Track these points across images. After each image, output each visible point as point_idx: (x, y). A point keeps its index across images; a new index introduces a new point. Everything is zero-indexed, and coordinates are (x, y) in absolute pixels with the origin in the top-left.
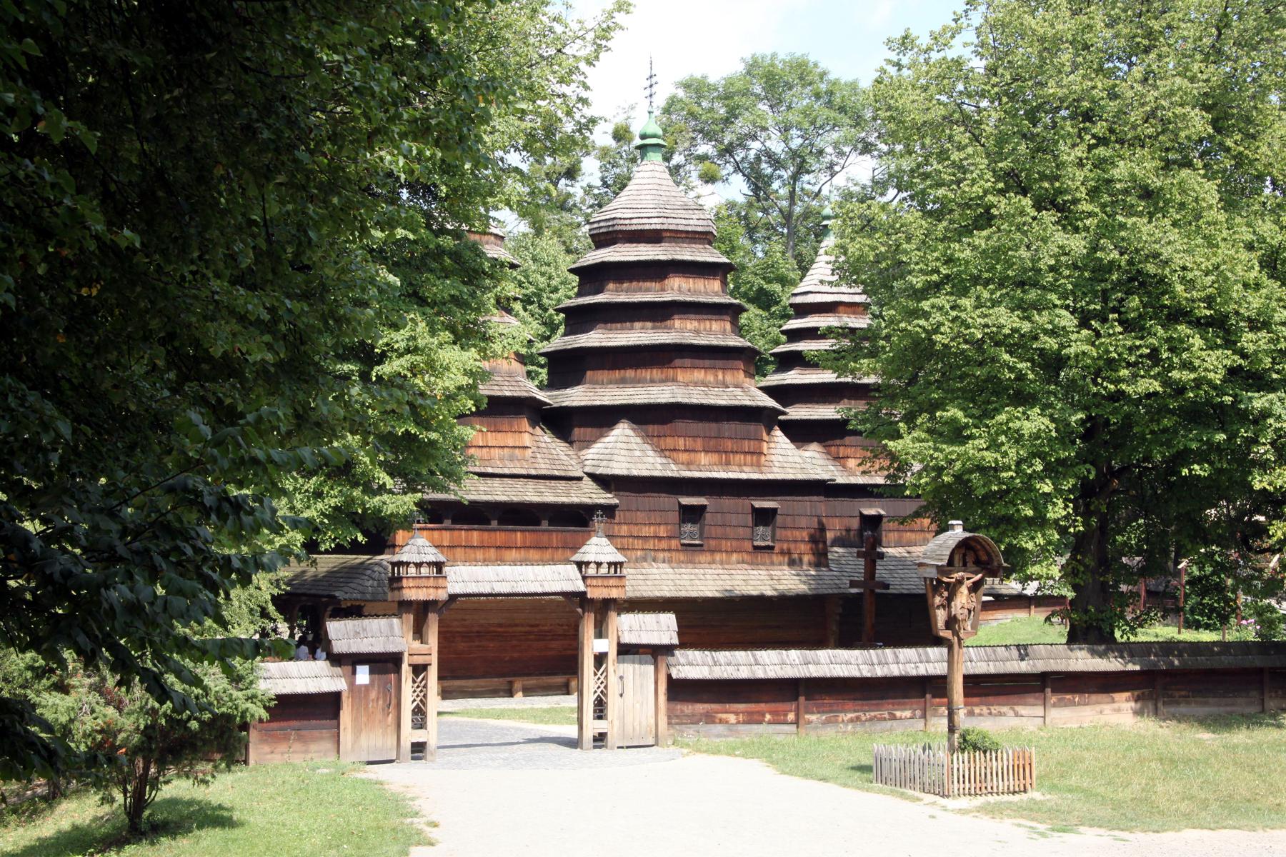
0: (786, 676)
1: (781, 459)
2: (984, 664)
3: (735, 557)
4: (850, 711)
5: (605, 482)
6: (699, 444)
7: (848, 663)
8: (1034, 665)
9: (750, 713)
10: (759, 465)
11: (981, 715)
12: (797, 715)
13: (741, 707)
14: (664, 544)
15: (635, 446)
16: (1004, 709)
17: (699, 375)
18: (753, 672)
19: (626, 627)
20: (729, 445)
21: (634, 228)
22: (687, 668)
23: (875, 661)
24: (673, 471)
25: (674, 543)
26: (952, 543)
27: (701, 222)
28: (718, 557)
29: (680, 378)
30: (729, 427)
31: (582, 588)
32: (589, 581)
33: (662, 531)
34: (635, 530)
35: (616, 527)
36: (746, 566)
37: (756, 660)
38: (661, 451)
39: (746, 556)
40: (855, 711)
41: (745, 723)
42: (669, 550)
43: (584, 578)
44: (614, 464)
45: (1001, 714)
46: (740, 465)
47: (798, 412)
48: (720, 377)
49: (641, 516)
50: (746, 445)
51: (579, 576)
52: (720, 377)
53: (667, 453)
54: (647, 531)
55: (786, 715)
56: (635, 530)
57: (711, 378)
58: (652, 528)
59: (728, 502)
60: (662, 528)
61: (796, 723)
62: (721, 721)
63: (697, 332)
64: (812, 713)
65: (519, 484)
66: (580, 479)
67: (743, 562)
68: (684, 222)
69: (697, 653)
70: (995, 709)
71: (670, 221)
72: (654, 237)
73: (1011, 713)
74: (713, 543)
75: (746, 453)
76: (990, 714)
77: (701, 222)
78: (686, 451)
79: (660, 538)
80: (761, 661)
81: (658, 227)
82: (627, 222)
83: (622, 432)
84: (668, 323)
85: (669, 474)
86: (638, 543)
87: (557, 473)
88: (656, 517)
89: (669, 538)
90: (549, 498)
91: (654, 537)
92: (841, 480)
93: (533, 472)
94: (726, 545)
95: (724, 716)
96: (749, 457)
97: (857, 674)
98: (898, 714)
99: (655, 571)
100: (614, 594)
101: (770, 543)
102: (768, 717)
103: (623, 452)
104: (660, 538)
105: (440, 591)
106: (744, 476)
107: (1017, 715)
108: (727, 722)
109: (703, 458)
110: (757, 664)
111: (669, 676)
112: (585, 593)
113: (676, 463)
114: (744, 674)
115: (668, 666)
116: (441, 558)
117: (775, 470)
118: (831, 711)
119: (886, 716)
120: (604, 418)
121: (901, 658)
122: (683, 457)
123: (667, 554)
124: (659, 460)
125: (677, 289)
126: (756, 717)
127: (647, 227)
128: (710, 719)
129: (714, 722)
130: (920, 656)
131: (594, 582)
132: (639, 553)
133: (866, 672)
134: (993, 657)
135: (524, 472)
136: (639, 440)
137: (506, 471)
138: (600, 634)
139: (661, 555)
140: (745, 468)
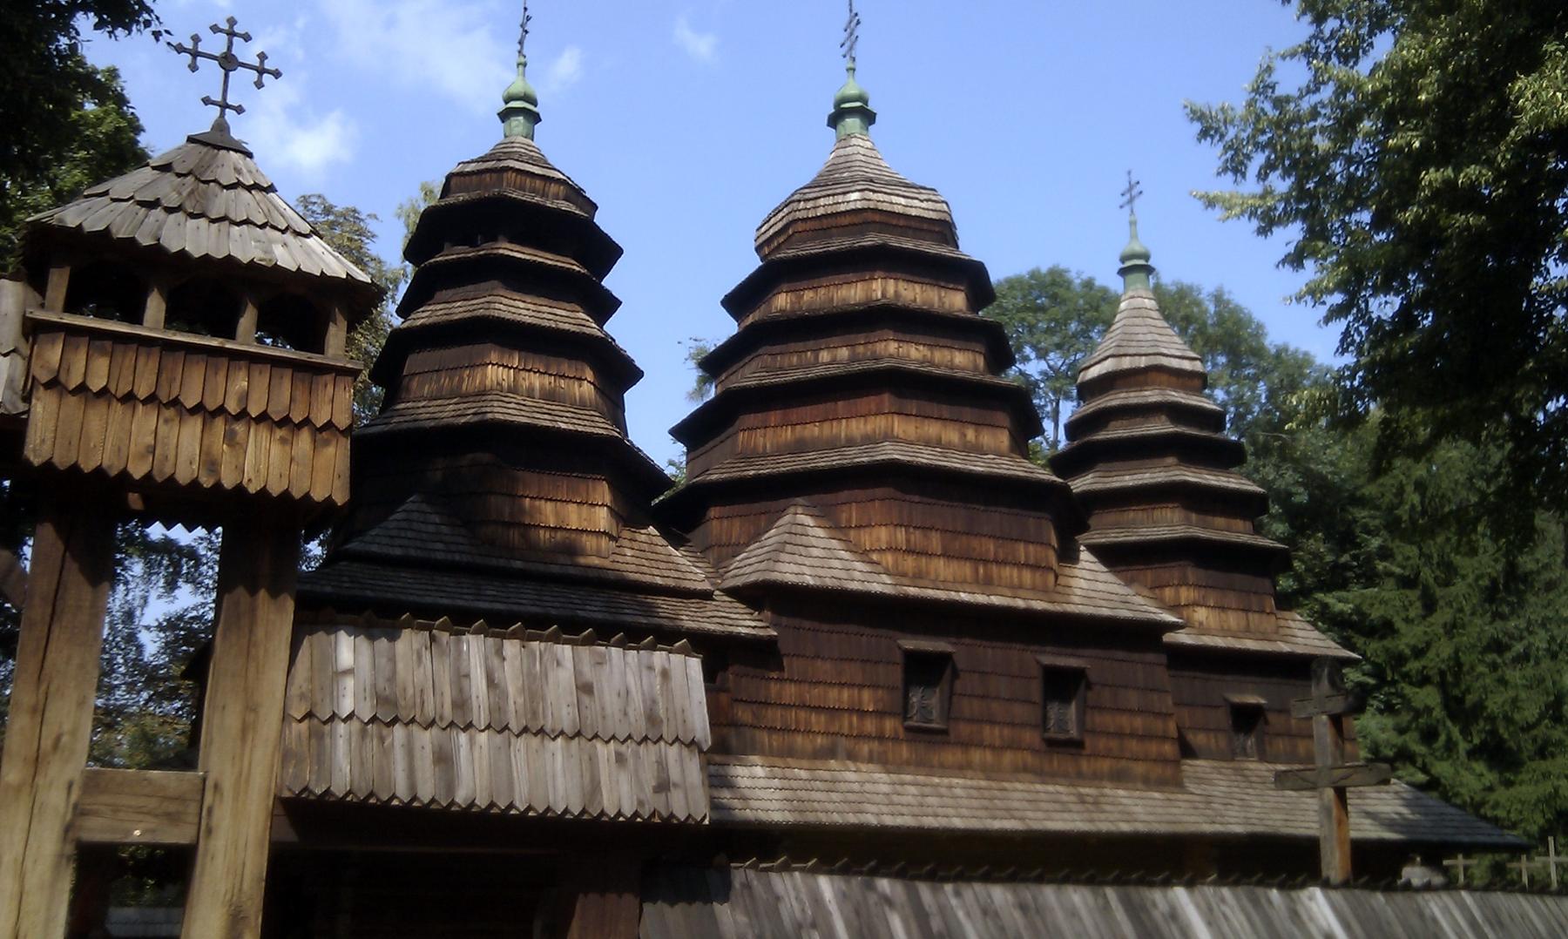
1: (1083, 584)
3: (1008, 758)
6: (936, 541)
10: (1045, 591)
14: (870, 726)
15: (814, 541)
21: (820, 212)
24: (881, 585)
25: (890, 725)
28: (977, 756)
30: (996, 518)
33: (868, 699)
34: (814, 694)
36: (1030, 777)
38: (863, 554)
39: (1029, 758)
42: (880, 738)
46: (1012, 587)
49: (824, 668)
53: (875, 557)
54: (835, 696)
56: (814, 694)
57: (951, 434)
58: (846, 694)
59: (991, 653)
66: (706, 596)
67: (1025, 769)
68: (903, 201)
69: (826, 886)
71: (881, 197)
74: (964, 730)
78: (909, 551)
79: (862, 713)
81: (859, 205)
82: (809, 205)
85: (876, 588)
86: (818, 721)
87: (659, 581)
88: (852, 671)
89: (879, 714)
91: (850, 711)
94: (991, 733)
96: (1027, 576)
101: (1074, 733)
104: (862, 713)
109: (942, 568)
117: (1076, 599)
122: (909, 563)
123: (875, 745)
124: (859, 565)
127: (842, 208)
132: (819, 740)
136: (820, 532)
139: (865, 748)
140: (1021, 593)
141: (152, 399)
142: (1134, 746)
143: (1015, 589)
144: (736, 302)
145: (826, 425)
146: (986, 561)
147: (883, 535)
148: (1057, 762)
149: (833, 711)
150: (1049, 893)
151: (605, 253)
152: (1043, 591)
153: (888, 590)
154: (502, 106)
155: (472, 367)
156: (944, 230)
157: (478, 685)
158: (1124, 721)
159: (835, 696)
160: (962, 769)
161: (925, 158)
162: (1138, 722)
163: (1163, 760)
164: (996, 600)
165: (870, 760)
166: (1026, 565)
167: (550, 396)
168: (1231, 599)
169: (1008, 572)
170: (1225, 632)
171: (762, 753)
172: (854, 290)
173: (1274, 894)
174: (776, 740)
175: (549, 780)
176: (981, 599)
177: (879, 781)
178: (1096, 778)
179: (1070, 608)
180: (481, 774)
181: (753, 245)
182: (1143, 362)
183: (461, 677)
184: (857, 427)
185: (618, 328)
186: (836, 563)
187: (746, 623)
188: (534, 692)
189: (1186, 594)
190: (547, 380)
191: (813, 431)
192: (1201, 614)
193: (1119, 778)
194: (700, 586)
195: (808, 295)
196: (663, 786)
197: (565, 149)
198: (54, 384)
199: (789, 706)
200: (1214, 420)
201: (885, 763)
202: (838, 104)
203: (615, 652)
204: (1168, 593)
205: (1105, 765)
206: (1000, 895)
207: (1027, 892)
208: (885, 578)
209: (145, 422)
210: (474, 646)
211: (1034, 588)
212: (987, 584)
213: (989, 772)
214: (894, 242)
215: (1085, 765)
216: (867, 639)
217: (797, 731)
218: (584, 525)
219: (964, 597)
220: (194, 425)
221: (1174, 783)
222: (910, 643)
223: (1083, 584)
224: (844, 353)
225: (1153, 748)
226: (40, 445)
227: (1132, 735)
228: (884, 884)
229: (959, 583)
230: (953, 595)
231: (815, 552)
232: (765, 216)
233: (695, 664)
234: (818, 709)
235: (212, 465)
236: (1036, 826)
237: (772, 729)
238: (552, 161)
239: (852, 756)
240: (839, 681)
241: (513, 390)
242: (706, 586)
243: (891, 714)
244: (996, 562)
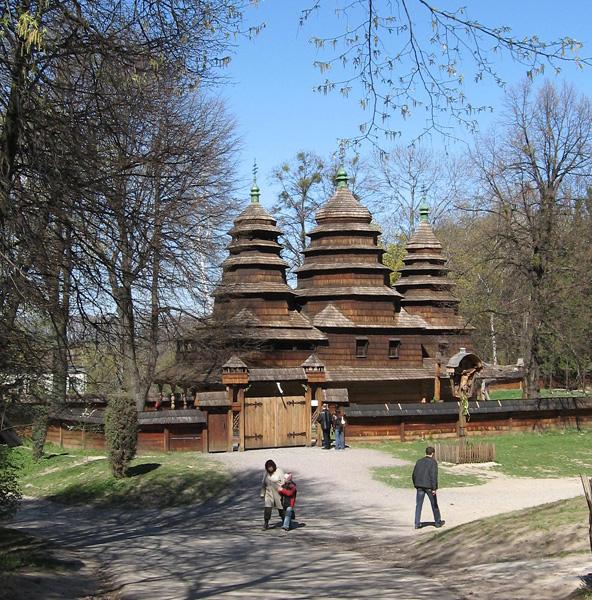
3: (380, 363)
5: (323, 329)
6: (364, 312)
20: (378, 312)
24: (351, 325)
26: (461, 358)
28: (373, 363)
33: (348, 351)
38: (347, 316)
47: (410, 297)
54: (342, 351)
59: (377, 338)
66: (311, 329)
74: (371, 356)
83: (330, 307)
92: (428, 328)
94: (376, 357)
100: (320, 380)
114: (378, 413)
122: (357, 318)
138: (313, 398)
139: (347, 362)
142: (411, 358)
147: (351, 312)
148: (394, 363)
152: (391, 323)
158: (409, 352)
159: (342, 351)
162: (412, 352)
176: (375, 326)
177: (350, 369)
182: (423, 246)
187: (321, 337)
189: (430, 315)
192: (433, 320)
200: (442, 262)
205: (404, 363)
212: (376, 322)
215: (399, 363)
216: (348, 337)
222: (357, 338)
224: (341, 259)
225: (416, 358)
240: (341, 344)
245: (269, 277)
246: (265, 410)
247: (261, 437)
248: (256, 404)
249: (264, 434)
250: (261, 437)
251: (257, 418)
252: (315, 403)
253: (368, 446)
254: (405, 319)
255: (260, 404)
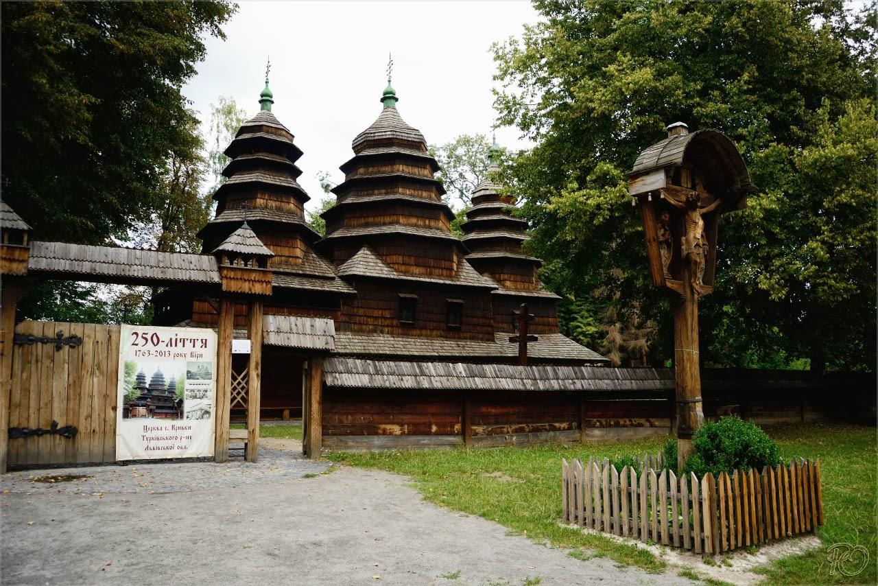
0: (452, 387)
1: (465, 274)
2: (628, 382)
3: (435, 332)
4: (514, 423)
5: (349, 279)
6: (412, 260)
7: (512, 377)
8: (665, 384)
9: (415, 425)
11: (624, 426)
12: (463, 427)
13: (406, 418)
14: (388, 322)
15: (370, 260)
16: (643, 421)
17: (414, 221)
18: (418, 383)
19: (272, 328)
21: (376, 138)
22: (345, 376)
23: (537, 376)
24: (394, 275)
25: (395, 322)
27: (417, 137)
29: (401, 221)
31: (216, 279)
32: (225, 272)
35: (355, 310)
37: (422, 371)
38: (388, 264)
40: (519, 423)
41: (410, 434)
42: (392, 326)
43: (220, 269)
44: (355, 269)
45: (640, 425)
46: (439, 276)
48: (427, 223)
50: (444, 264)
51: (215, 268)
52: (427, 223)
54: (376, 313)
55: (452, 427)
56: (369, 312)
57: (421, 223)
58: (380, 312)
60: (387, 312)
61: (463, 433)
62: (385, 433)
63: (411, 195)
64: (479, 425)
65: (288, 279)
66: (333, 279)
70: (636, 421)
72: (389, 142)
73: (648, 424)
74: (421, 323)
75: (442, 269)
76: (632, 425)
77: (417, 137)
78: (403, 264)
80: (427, 371)
84: (396, 190)
85: (392, 277)
86: (370, 321)
89: (392, 318)
90: (308, 286)
93: (301, 272)
95: (388, 427)
96: (444, 272)
97: (521, 387)
98: (557, 425)
99: (382, 338)
102: (434, 428)
103: (361, 263)
105: (15, 265)
106: (442, 282)
107: (652, 426)
108: (391, 434)
109: (416, 270)
110: (423, 374)
111: (324, 383)
112: (220, 285)
113: (396, 271)
114: (409, 383)
115: (323, 374)
116: (22, 225)
118: (497, 423)
119: (547, 427)
120: (352, 246)
121: (560, 373)
122: (403, 268)
123: (390, 328)
124: (386, 269)
125: (402, 170)
126: (423, 428)
127: (384, 137)
128: (372, 430)
129: (377, 434)
130: (576, 373)
131: (232, 275)
133: (529, 385)
134: (634, 376)
135: (294, 271)
136: (373, 257)
137: (281, 270)
139: (386, 330)
141: (241, 279)
143: (439, 276)
144: (345, 168)
145: (376, 219)
146: (430, 267)
149: (376, 318)
150: (402, 363)
151: (297, 153)
152: (450, 277)
153: (396, 277)
154: (260, 98)
155: (251, 199)
156: (419, 144)
157: (293, 326)
159: (376, 313)
160: (419, 336)
161: (414, 115)
163: (489, 333)
164: (433, 280)
165: (388, 333)
166: (445, 268)
167: (279, 209)
168: (519, 278)
169: (437, 271)
170: (516, 289)
171: (351, 331)
172: (388, 166)
173: (451, 364)
174: (356, 327)
175: (307, 343)
176: (428, 280)
177: (390, 339)
178: (465, 338)
179: (458, 283)
180: (294, 341)
181: (351, 147)
183: (291, 324)
184: (387, 219)
185: (302, 182)
186: (378, 268)
188: (304, 326)
190: (277, 203)
191: (371, 220)
192: (508, 283)
193: (472, 338)
194: (331, 275)
195: (371, 169)
196: (327, 343)
197: (282, 113)
198: (226, 277)
199: (361, 316)
201: (392, 334)
202: (385, 94)
203: (317, 319)
204: (497, 276)
206: (392, 363)
207: (397, 363)
208: (395, 273)
209: (240, 283)
210: (293, 319)
211: (447, 276)
212: (430, 275)
213: (427, 337)
214: (403, 151)
217: (363, 324)
218: (291, 255)
219: (422, 279)
220: (247, 282)
221: (492, 340)
222: (402, 295)
223: (465, 274)
224: (383, 191)
226: (224, 288)
227: (478, 325)
228: (368, 361)
229: (420, 275)
230: (418, 279)
231: (371, 264)
232: (356, 136)
233: (332, 321)
234: (370, 317)
235: (250, 290)
236: (441, 354)
237: (355, 323)
238: (281, 123)
239: (382, 332)
241: (266, 207)
242: (333, 275)
243: (395, 318)
244: (434, 267)
245: (272, 204)
246: (89, 359)
247: (70, 432)
248: (59, 342)
249: (82, 428)
250: (70, 432)
251: (59, 384)
252: (242, 346)
253: (369, 463)
254: (470, 277)
255: (75, 342)
